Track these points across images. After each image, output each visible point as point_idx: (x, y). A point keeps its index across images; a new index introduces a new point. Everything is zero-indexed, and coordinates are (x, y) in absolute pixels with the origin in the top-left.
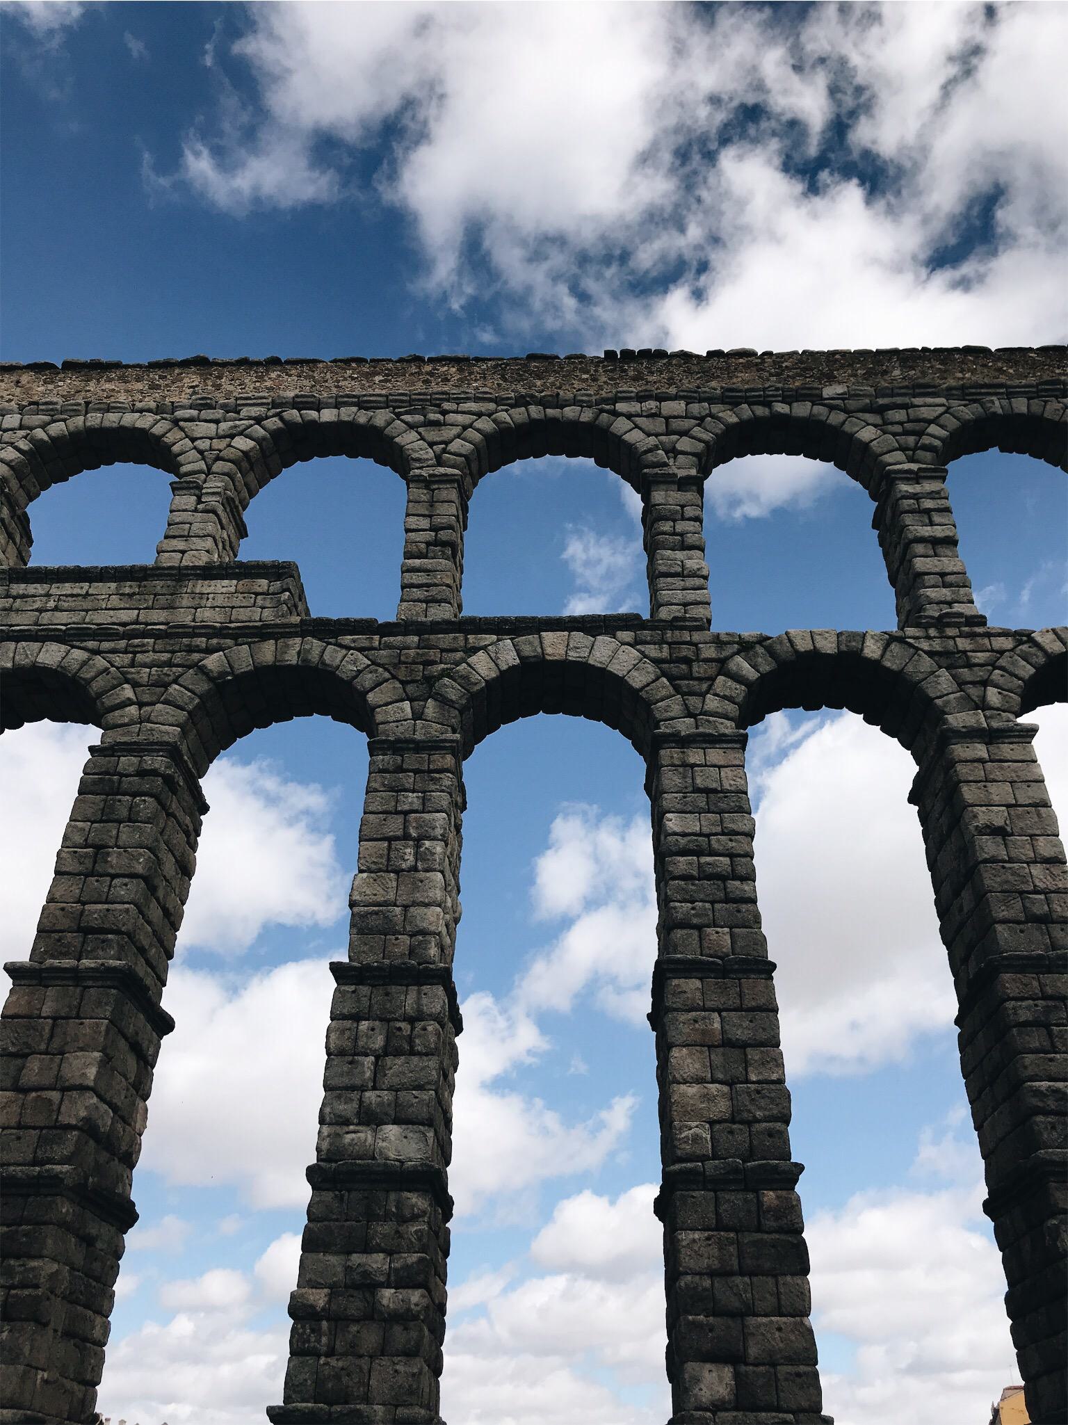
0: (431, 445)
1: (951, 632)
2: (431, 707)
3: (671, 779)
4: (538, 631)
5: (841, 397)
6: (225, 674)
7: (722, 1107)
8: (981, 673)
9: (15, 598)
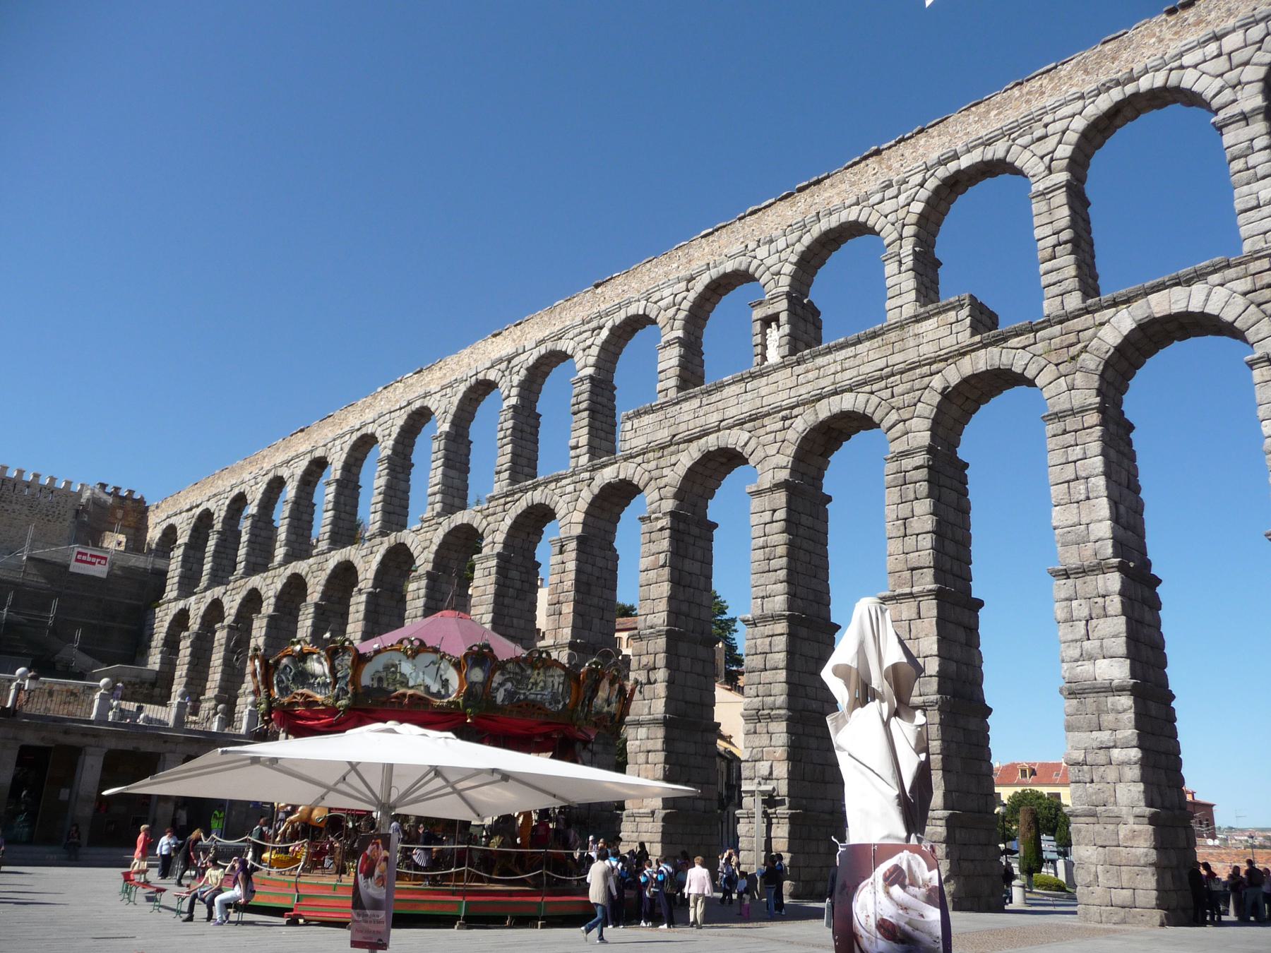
0: (1042, 158)
4: (1147, 294)
6: (945, 389)
9: (819, 369)
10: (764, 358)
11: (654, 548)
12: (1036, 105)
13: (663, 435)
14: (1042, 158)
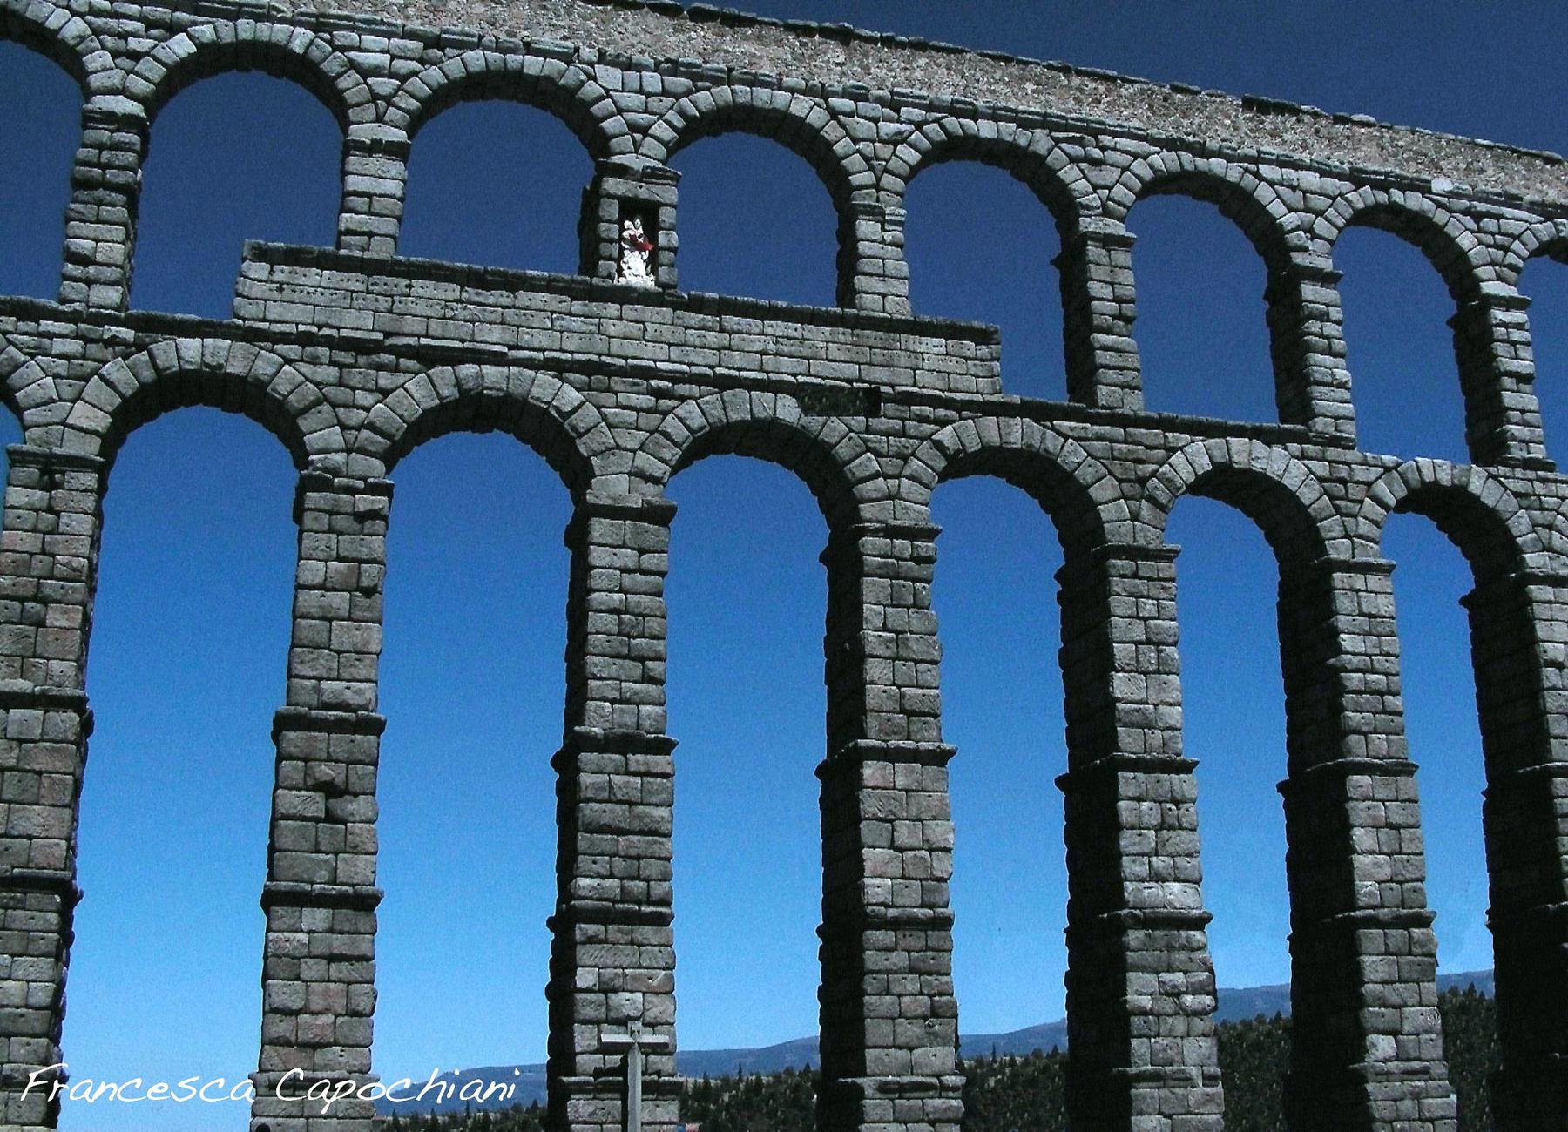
0: (1095, 187)
1: (1531, 474)
2: (1146, 508)
3: (1343, 602)
5: (1449, 194)
6: (958, 452)
7: (1386, 872)
8: (1547, 517)
9: (731, 332)
10: (620, 272)
11: (347, 544)
12: (1096, 114)
13: (359, 323)
14: (1095, 187)
